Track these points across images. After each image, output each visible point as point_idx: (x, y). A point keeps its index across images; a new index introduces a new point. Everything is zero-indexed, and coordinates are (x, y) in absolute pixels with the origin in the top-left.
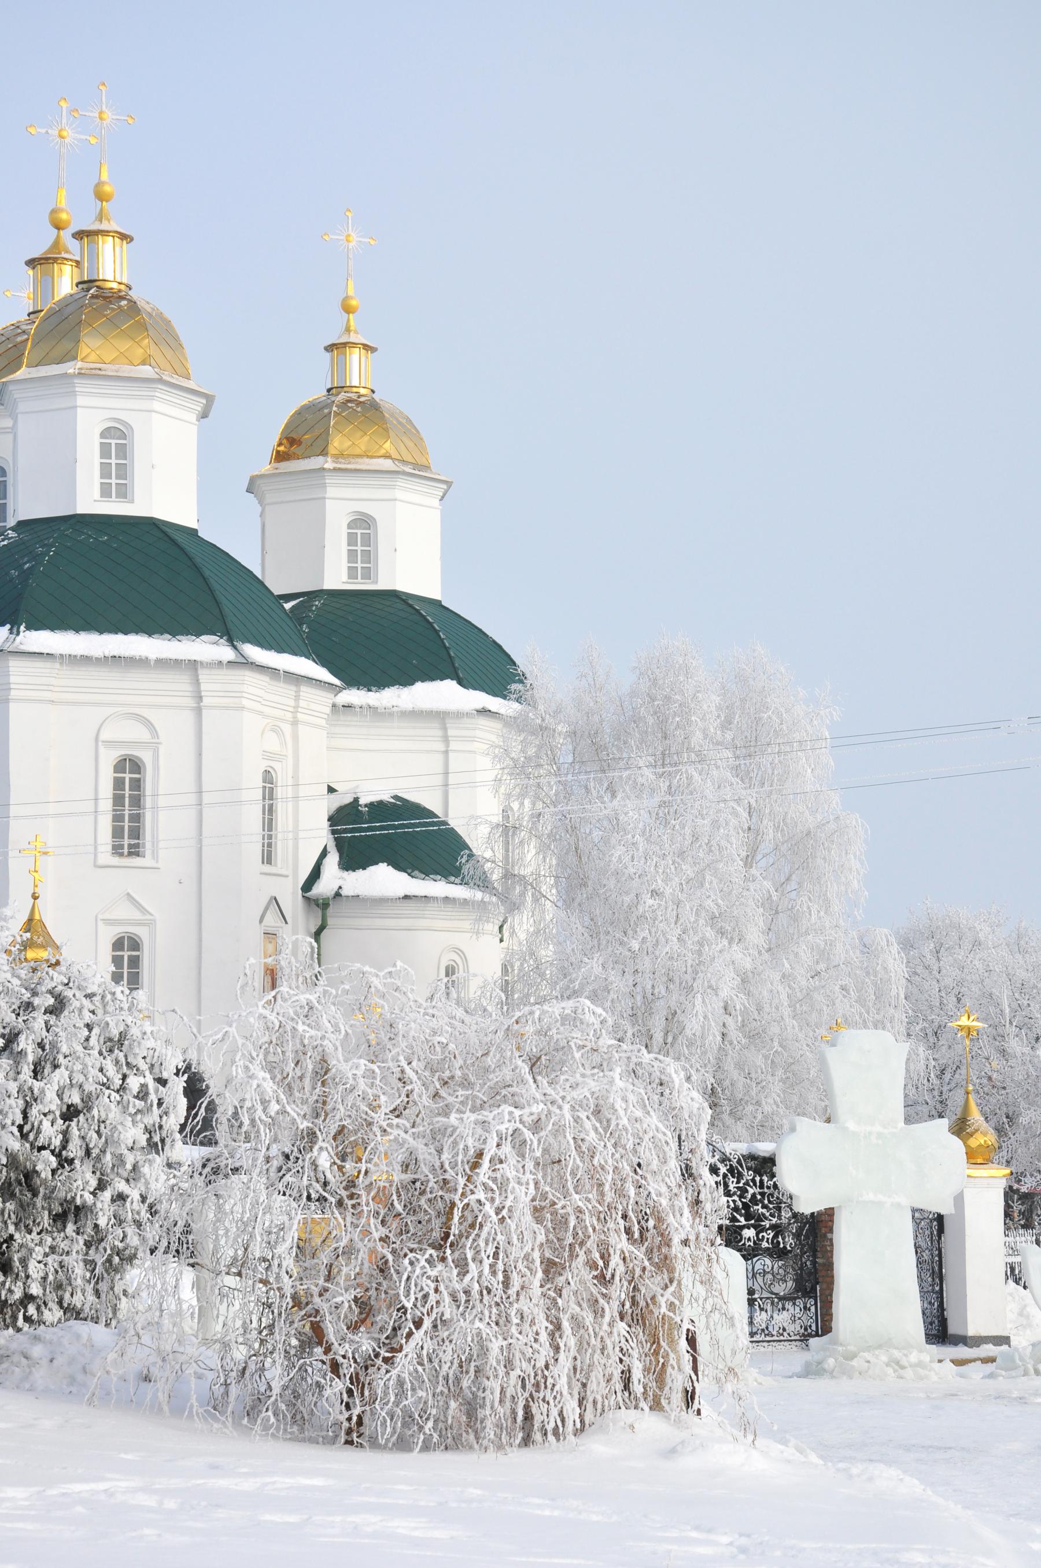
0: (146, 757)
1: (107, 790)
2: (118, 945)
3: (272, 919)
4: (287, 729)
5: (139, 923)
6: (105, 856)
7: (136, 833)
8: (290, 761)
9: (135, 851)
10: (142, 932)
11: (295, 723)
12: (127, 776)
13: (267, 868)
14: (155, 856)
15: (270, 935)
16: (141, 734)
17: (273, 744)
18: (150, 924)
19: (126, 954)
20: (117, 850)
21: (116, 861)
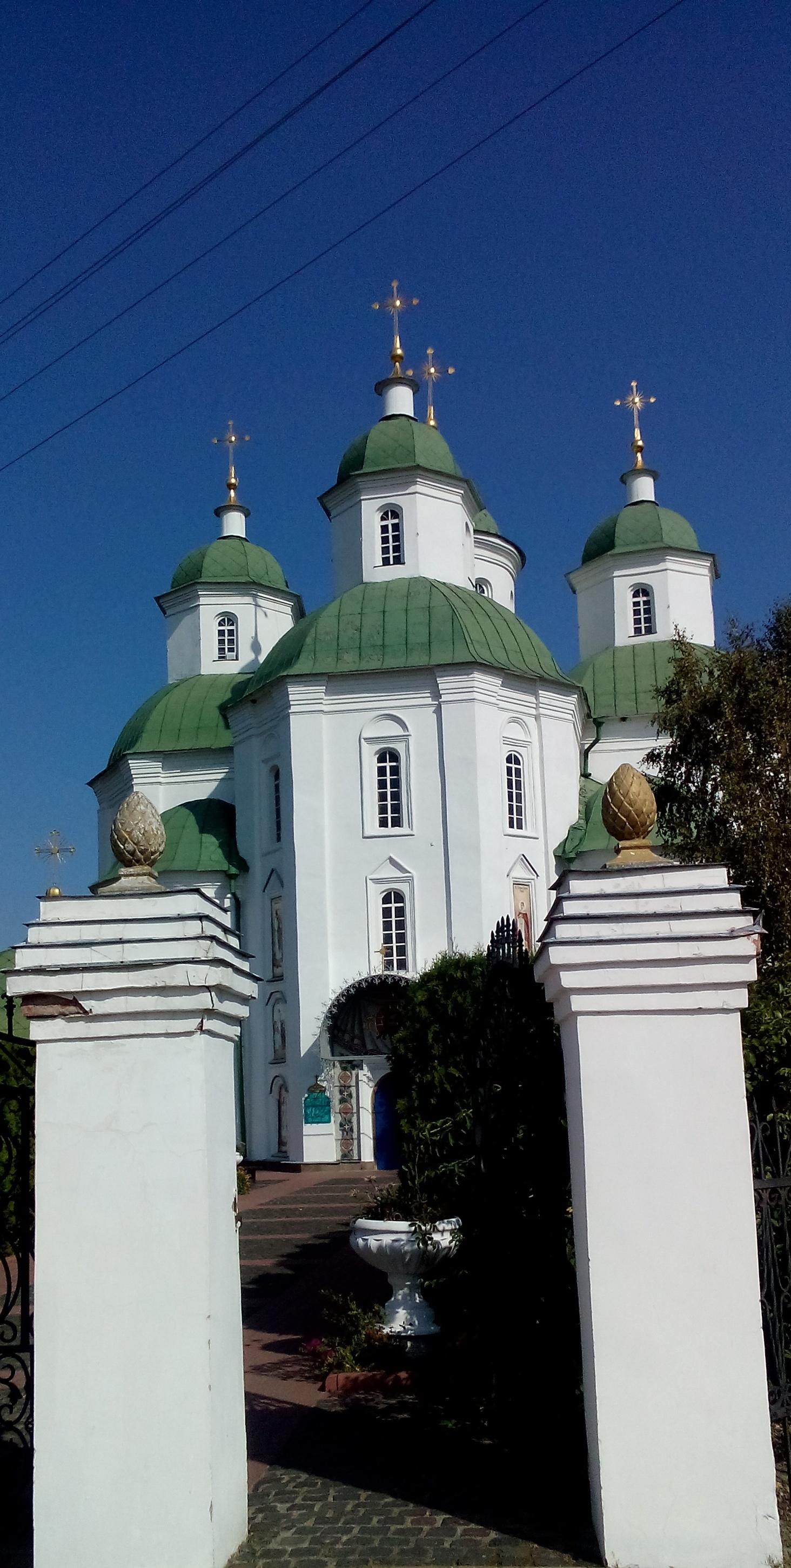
0: (400, 747)
1: (371, 779)
2: (386, 900)
3: (521, 873)
4: (531, 722)
5: (398, 880)
6: (372, 827)
7: (397, 809)
8: (536, 744)
9: (397, 823)
10: (404, 888)
11: (537, 717)
12: (388, 765)
13: (515, 831)
14: (410, 825)
15: (519, 884)
16: (393, 729)
17: (516, 732)
18: (410, 880)
19: (393, 906)
20: (383, 823)
21: (384, 831)
